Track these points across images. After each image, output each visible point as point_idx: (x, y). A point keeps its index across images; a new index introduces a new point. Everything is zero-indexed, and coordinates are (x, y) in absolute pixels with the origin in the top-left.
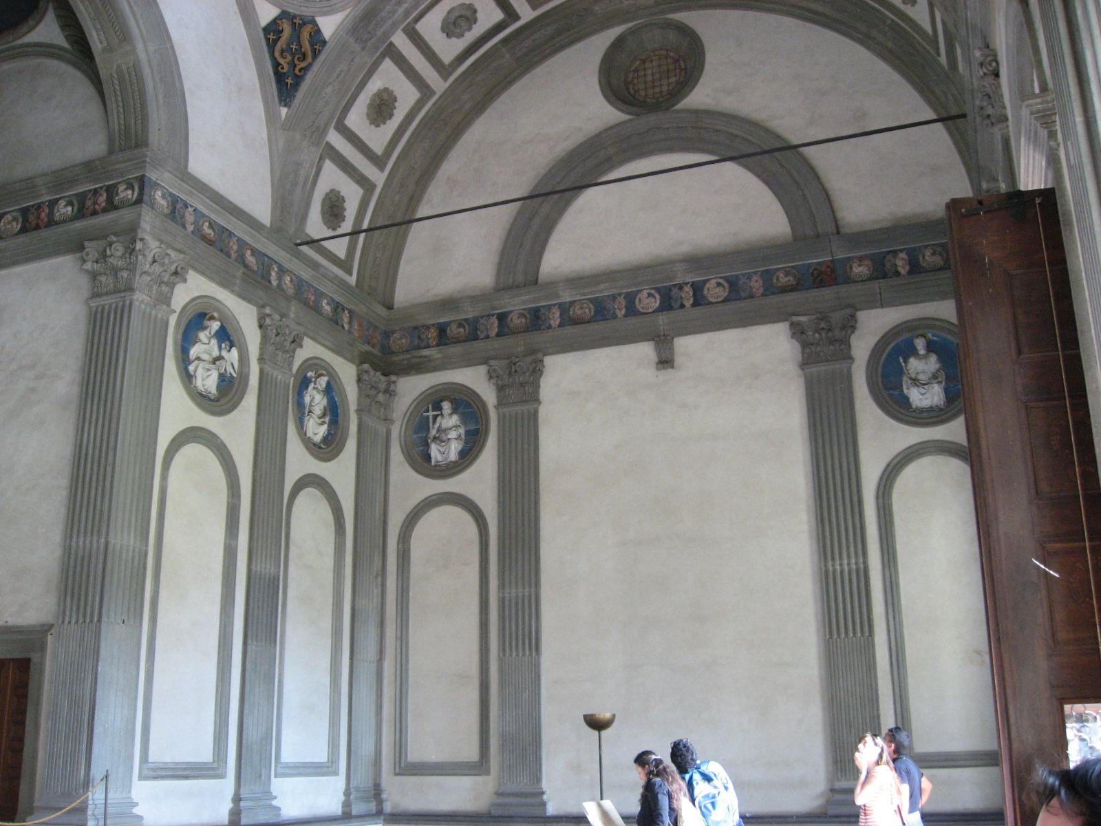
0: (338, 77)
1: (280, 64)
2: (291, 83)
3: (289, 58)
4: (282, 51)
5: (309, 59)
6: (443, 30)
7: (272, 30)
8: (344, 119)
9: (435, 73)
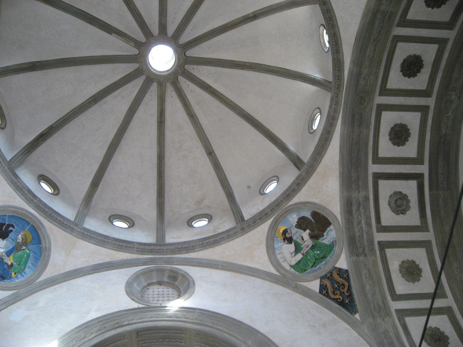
0: (366, 278)
1: (338, 298)
2: (349, 302)
3: (338, 292)
4: (333, 292)
5: (346, 284)
6: (398, 214)
7: (323, 288)
8: (396, 293)
9: (418, 233)
